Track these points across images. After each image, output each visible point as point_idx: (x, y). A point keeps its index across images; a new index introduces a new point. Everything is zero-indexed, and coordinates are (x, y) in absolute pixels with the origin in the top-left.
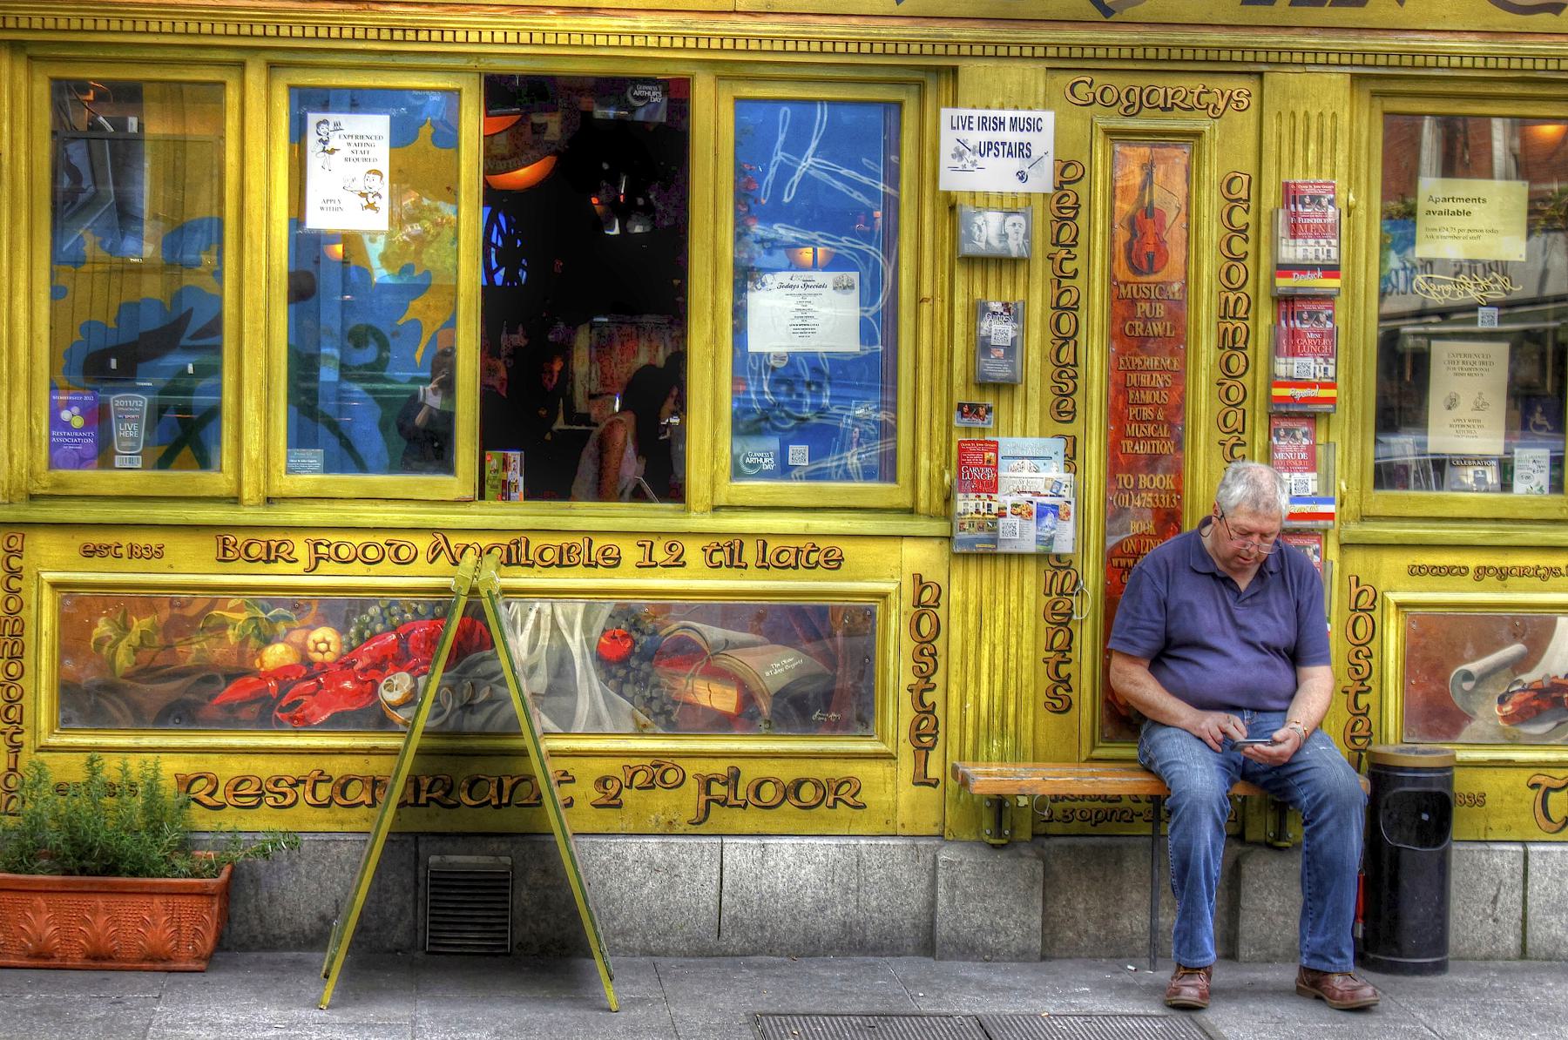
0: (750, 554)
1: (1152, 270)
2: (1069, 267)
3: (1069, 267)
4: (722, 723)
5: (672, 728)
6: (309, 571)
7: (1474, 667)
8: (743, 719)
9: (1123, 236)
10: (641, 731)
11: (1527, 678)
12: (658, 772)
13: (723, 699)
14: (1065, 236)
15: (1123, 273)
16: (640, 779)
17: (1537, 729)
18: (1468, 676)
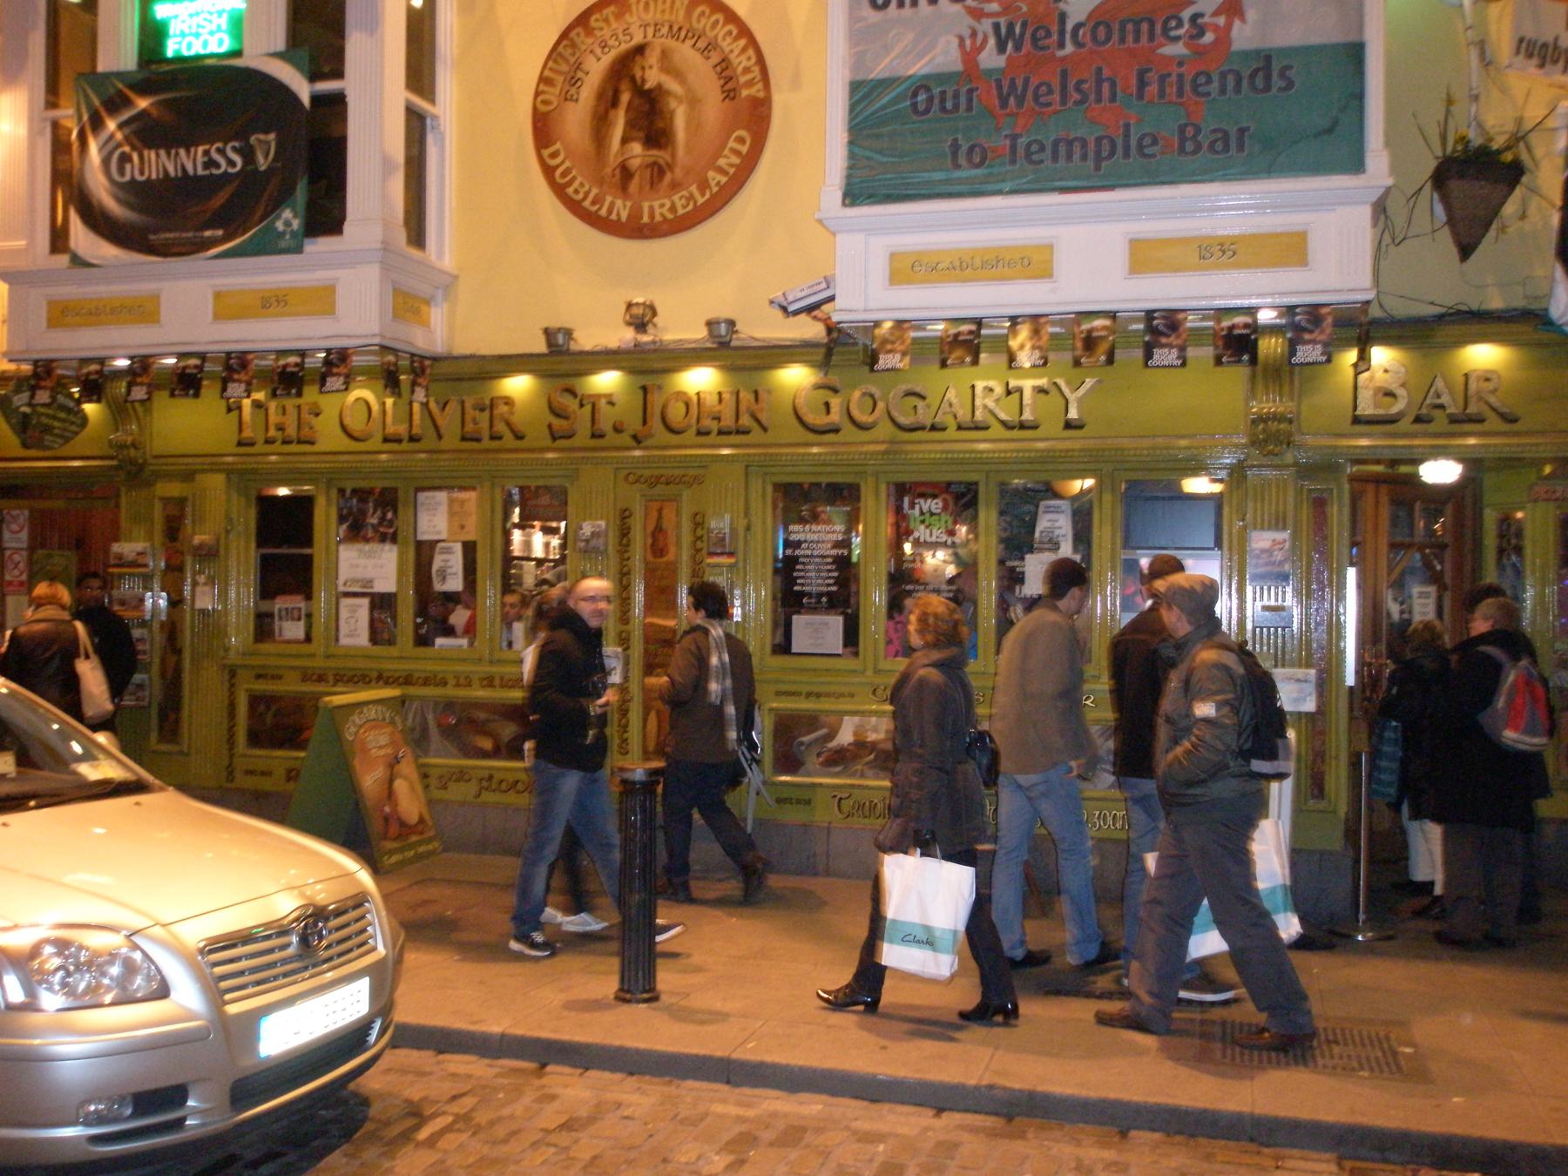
0: (497, 682)
1: (662, 555)
2: (626, 555)
3: (626, 555)
4: (485, 755)
5: (467, 755)
6: (334, 685)
7: (805, 739)
8: (496, 753)
9: (650, 541)
10: (454, 757)
11: (833, 744)
12: (461, 776)
13: (487, 744)
14: (624, 541)
15: (650, 558)
16: (454, 777)
17: (838, 769)
18: (802, 743)
